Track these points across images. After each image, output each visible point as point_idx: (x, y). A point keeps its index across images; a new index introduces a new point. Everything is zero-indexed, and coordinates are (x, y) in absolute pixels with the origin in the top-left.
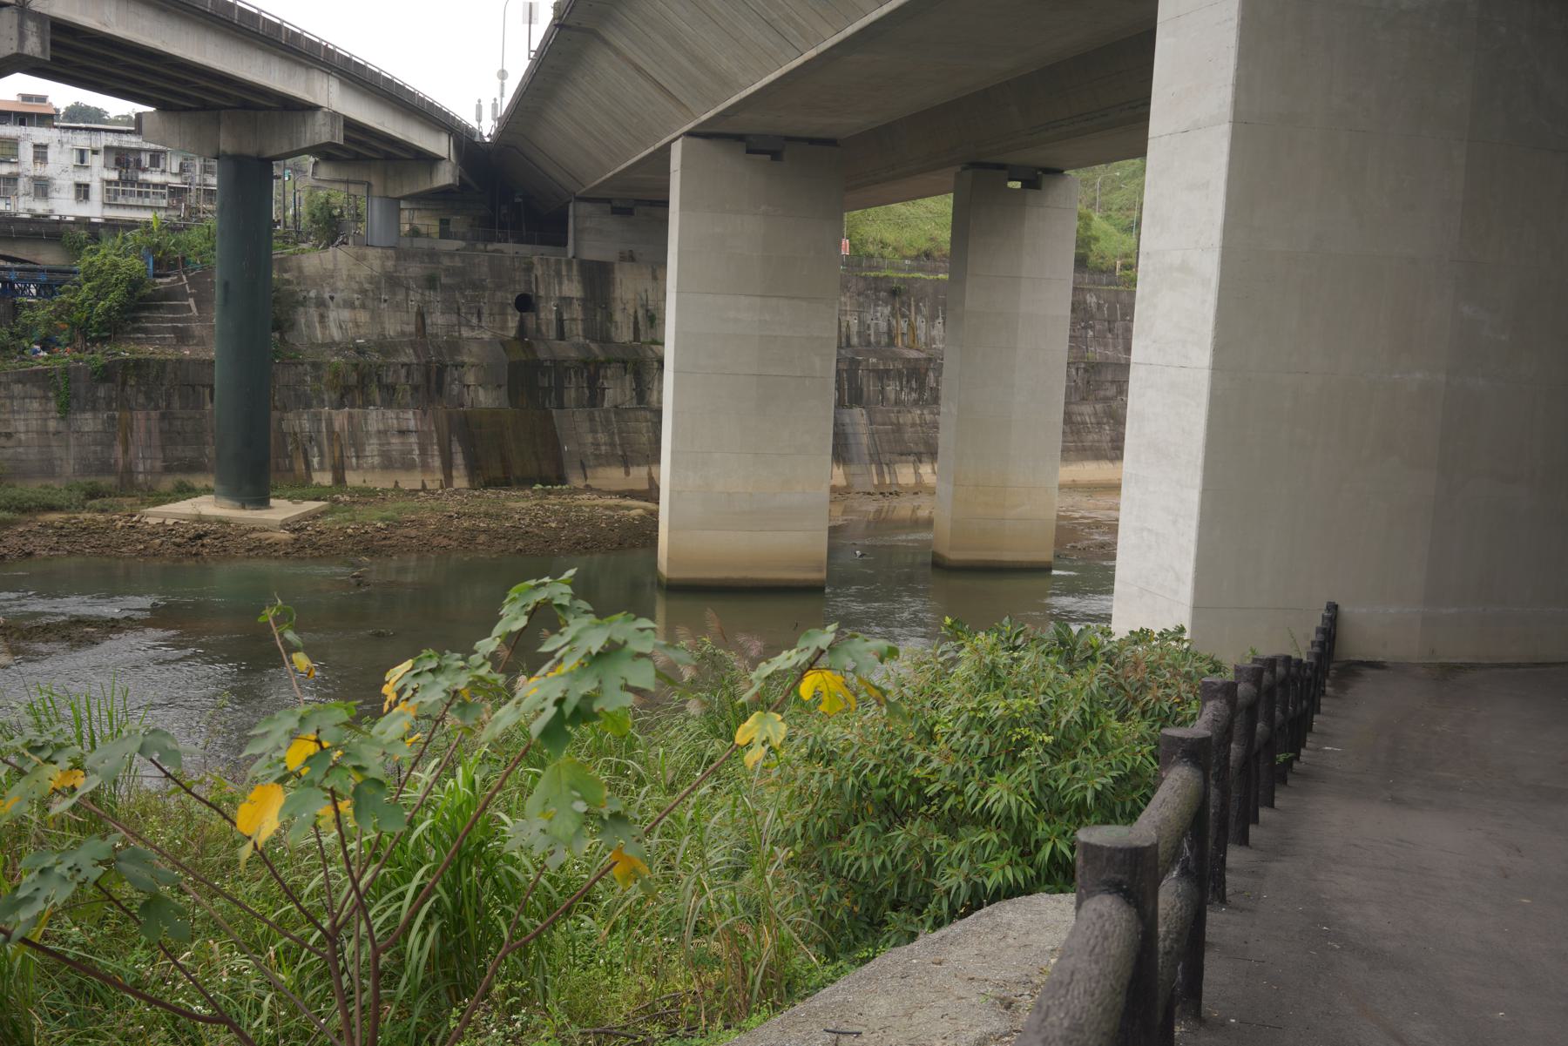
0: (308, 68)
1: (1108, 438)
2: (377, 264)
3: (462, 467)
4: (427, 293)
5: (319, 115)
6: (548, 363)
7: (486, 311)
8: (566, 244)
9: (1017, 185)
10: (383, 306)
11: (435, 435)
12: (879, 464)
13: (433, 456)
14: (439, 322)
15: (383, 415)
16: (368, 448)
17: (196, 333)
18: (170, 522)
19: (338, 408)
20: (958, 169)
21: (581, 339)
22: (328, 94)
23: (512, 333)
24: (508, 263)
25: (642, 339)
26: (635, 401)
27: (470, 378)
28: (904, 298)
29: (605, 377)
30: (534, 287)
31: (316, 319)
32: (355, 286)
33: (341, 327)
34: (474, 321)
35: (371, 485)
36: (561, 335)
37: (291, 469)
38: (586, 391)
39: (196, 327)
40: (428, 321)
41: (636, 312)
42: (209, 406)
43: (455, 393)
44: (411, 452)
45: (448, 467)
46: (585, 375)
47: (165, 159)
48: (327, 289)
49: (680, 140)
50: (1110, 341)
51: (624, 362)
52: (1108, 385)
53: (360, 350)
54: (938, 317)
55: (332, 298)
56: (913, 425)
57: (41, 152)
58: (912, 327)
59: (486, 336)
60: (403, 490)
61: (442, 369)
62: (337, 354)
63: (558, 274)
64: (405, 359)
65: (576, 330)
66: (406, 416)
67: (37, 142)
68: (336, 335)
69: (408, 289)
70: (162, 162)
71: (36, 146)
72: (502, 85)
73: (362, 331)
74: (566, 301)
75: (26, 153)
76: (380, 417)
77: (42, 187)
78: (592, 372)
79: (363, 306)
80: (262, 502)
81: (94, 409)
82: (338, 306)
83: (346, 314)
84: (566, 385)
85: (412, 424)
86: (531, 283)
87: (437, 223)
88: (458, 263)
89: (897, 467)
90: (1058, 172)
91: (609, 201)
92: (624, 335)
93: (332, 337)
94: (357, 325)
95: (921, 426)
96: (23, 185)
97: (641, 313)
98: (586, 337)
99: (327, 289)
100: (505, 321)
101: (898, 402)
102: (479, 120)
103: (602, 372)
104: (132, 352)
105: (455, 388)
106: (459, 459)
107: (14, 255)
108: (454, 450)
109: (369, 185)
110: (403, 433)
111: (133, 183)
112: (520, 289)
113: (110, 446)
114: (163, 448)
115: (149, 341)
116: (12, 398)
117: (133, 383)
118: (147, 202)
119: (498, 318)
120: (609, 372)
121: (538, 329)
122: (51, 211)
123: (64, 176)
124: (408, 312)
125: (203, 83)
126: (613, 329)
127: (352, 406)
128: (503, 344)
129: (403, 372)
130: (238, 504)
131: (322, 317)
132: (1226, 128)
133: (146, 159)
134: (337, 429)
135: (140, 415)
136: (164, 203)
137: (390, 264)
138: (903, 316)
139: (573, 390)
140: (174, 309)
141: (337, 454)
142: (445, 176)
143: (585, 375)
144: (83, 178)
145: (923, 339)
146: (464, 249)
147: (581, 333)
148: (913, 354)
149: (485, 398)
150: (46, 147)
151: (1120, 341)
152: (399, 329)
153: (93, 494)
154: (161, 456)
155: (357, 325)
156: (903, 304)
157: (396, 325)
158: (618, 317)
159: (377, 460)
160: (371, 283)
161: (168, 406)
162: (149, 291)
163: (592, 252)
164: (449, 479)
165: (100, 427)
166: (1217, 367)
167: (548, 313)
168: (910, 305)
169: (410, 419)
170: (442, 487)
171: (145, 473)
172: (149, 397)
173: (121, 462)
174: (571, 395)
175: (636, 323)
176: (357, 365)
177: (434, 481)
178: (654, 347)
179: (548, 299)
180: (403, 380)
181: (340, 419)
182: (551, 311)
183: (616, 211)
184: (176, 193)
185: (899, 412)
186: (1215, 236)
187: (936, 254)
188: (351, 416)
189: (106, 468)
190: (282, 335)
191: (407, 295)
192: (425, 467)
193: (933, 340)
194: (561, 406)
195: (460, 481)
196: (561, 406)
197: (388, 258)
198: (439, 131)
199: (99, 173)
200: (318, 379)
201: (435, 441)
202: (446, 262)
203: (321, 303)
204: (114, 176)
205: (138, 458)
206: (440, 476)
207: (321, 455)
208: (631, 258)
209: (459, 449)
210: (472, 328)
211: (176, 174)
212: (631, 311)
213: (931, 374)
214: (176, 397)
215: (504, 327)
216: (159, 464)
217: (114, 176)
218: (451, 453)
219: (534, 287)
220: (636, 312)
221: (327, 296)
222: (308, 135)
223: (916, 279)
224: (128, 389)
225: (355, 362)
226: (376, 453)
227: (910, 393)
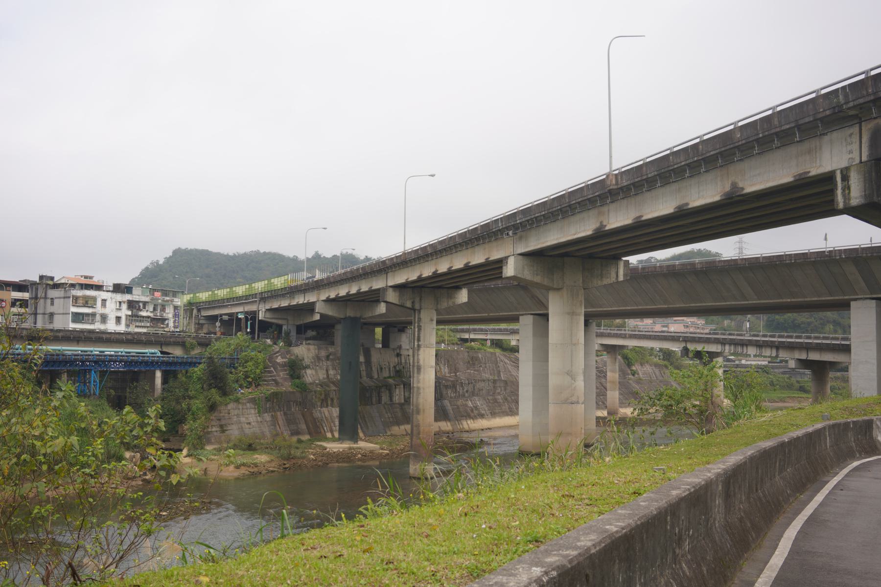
10: (318, 368)
12: (457, 420)
18: (341, 450)
37: (321, 432)
40: (329, 373)
57: (104, 301)
58: (440, 368)
67: (103, 298)
70: (147, 307)
71: (103, 300)
75: (99, 303)
77: (104, 319)
79: (313, 369)
80: (356, 442)
81: (266, 412)
89: (462, 421)
96: (98, 318)
111: (138, 316)
116: (247, 409)
118: (143, 324)
120: (383, 390)
123: (112, 313)
133: (141, 305)
136: (148, 325)
137: (317, 351)
144: (119, 314)
158: (373, 369)
172: (279, 407)
174: (374, 399)
199: (125, 312)
204: (130, 313)
211: (151, 312)
217: (130, 313)
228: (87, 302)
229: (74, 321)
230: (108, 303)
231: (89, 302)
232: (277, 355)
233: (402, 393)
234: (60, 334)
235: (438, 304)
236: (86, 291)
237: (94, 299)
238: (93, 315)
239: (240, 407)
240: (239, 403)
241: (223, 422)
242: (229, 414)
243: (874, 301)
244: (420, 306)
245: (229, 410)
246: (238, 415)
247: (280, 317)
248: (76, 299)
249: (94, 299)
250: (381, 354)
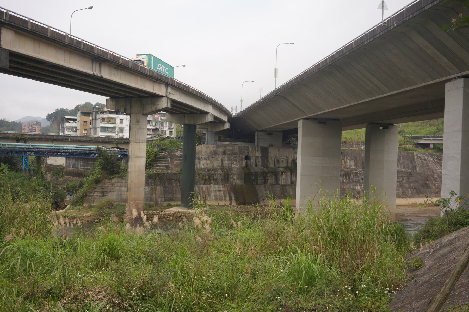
0: (208, 104)
1: (401, 192)
2: (212, 149)
3: (234, 200)
4: (224, 156)
5: (209, 115)
6: (254, 173)
7: (238, 160)
8: (254, 142)
9: (381, 128)
10: (213, 159)
11: (227, 192)
13: (227, 197)
14: (227, 163)
15: (215, 186)
16: (211, 195)
17: (171, 167)
18: (172, 213)
19: (204, 185)
20: (367, 124)
21: (261, 167)
22: (209, 109)
23: (244, 166)
24: (243, 148)
25: (276, 166)
26: (275, 183)
27: (235, 177)
28: (343, 155)
29: (268, 177)
30: (249, 154)
31: (198, 163)
32: (207, 154)
34: (235, 162)
35: (213, 204)
36: (256, 166)
38: (263, 180)
39: (171, 165)
40: (224, 163)
41: (274, 160)
42: (174, 185)
43: (231, 181)
44: (222, 196)
45: (231, 199)
46: (263, 176)
47: (151, 122)
48: (200, 155)
49: (301, 121)
50: (399, 165)
51: (273, 173)
52: (400, 177)
53: (208, 170)
54: (352, 160)
55: (201, 157)
56: (348, 189)
57: (121, 121)
59: (238, 166)
60: (220, 206)
61: (228, 175)
62: (203, 171)
63: (255, 151)
64: (219, 173)
65: (260, 164)
66: (220, 187)
67: (121, 119)
68: (203, 167)
69: (219, 155)
70: (150, 123)
71: (120, 120)
72: (241, 104)
73: (209, 166)
74: (257, 157)
75: (118, 121)
78: (264, 175)
79: (209, 159)
82: (203, 159)
83: (205, 161)
84: (258, 179)
85: (222, 189)
87: (218, 137)
88: (231, 148)
90: (392, 124)
91: (266, 131)
92: (271, 165)
94: (207, 164)
95: (350, 189)
96: (117, 129)
97: (276, 160)
98: (262, 166)
99: (200, 155)
100: (242, 162)
101: (343, 182)
102: (232, 112)
103: (267, 175)
104: (157, 171)
105: (231, 180)
106: (233, 198)
107: (122, 147)
108: (232, 195)
109: (208, 129)
110: (220, 191)
112: (246, 154)
113: (152, 194)
114: (164, 195)
115: (160, 168)
117: (157, 179)
119: (240, 162)
121: (250, 164)
122: (124, 136)
123: (127, 127)
124: (219, 160)
125: (186, 108)
126: (269, 164)
127: (207, 184)
128: (242, 168)
129: (219, 176)
130: (187, 209)
131: (199, 162)
132: (461, 132)
134: (204, 190)
135: (159, 187)
136: (151, 133)
137: (215, 149)
138: (343, 159)
139: (260, 180)
140: (165, 161)
141: (204, 197)
142: (227, 126)
143: (263, 176)
145: (348, 166)
146: (229, 144)
147: (261, 165)
148: (346, 170)
149: (238, 182)
150: (123, 120)
151: (402, 165)
152: (217, 165)
153: (151, 206)
154: (164, 197)
155: (207, 164)
156: (343, 156)
157: (216, 164)
158: (270, 161)
159: (214, 198)
160: (210, 153)
161: (165, 185)
162: (159, 156)
163: (262, 145)
164: (231, 203)
165: (150, 190)
166: (461, 175)
167: (253, 160)
168: (345, 157)
169: (221, 187)
170: (229, 205)
171: (161, 201)
172: (160, 183)
173: (155, 198)
174: (259, 181)
175: (274, 163)
176: (208, 174)
177: (227, 203)
178: (279, 168)
179: (253, 157)
180: (219, 178)
181: (205, 187)
183: (268, 134)
184: (154, 131)
185: (344, 185)
186: (460, 152)
187: (347, 142)
188: (207, 187)
189: (151, 200)
191: (219, 156)
192: (225, 200)
193: (351, 166)
194: (257, 184)
195: (234, 203)
196: (257, 184)
197: (214, 147)
198: (226, 115)
200: (199, 178)
201: (227, 193)
202: (228, 148)
205: (158, 197)
206: (229, 202)
207: (201, 197)
208: (272, 146)
209: (233, 195)
210: (234, 164)
212: (273, 160)
213: (352, 175)
214: (167, 182)
215: (242, 164)
216: (163, 199)
218: (231, 196)
219: (249, 154)
220: (274, 160)
221: (200, 157)
222: (206, 119)
223: (346, 149)
224: (156, 180)
225: (208, 173)
226: (213, 196)
227: (346, 180)
228: (110, 121)
229: (101, 132)
230: (124, 121)
231: (111, 121)
232: (178, 150)
233: (289, 178)
234: (36, 137)
235: (144, 109)
236: (109, 114)
237: (115, 119)
238: (114, 128)
239: (124, 181)
240: (123, 179)
241: (105, 190)
242: (113, 185)
243: (462, 80)
244: (131, 112)
245: (113, 183)
246: (120, 186)
247: (201, 127)
248: (103, 119)
249: (115, 119)
250: (279, 151)
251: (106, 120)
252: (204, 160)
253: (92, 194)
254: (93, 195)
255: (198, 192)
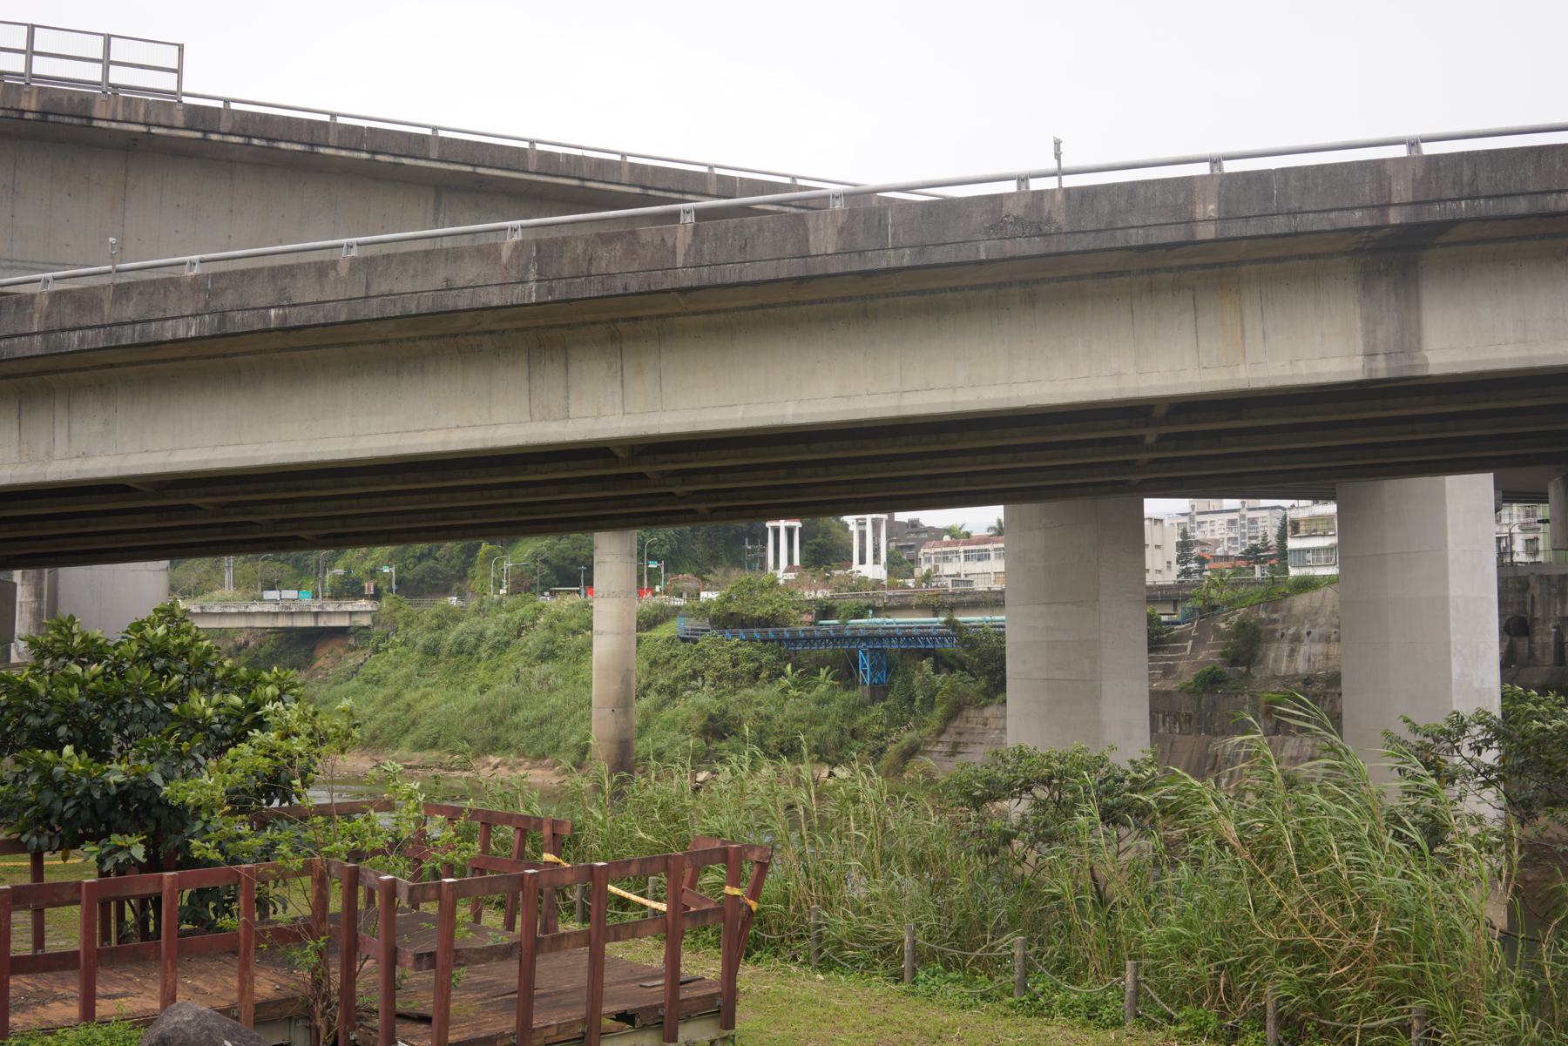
30: (1529, 608)
33: (1309, 660)
76: (1297, 744)
82: (1313, 641)
83: (1319, 648)
86: (1525, 603)
93: (1296, 669)
131: (1293, 651)
140: (1175, 650)
179: (1546, 620)
182: (1549, 633)
190: (1249, 669)
203: (1297, 639)
219: (1529, 608)
241: (963, 739)
242: (986, 725)
245: (987, 719)
251: (1302, 528)
252: (1319, 641)
253: (929, 748)
254: (931, 751)
255: (1228, 760)
